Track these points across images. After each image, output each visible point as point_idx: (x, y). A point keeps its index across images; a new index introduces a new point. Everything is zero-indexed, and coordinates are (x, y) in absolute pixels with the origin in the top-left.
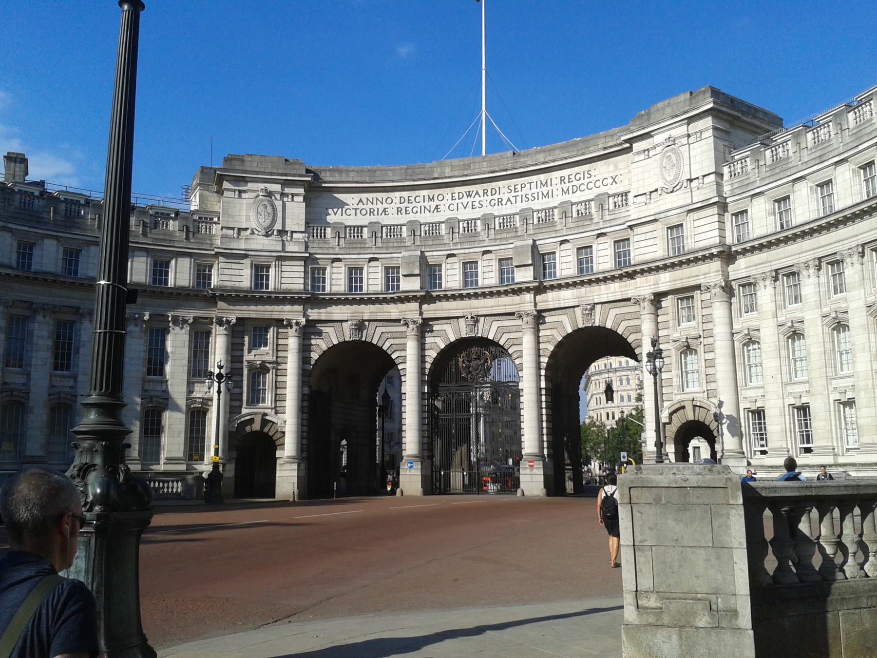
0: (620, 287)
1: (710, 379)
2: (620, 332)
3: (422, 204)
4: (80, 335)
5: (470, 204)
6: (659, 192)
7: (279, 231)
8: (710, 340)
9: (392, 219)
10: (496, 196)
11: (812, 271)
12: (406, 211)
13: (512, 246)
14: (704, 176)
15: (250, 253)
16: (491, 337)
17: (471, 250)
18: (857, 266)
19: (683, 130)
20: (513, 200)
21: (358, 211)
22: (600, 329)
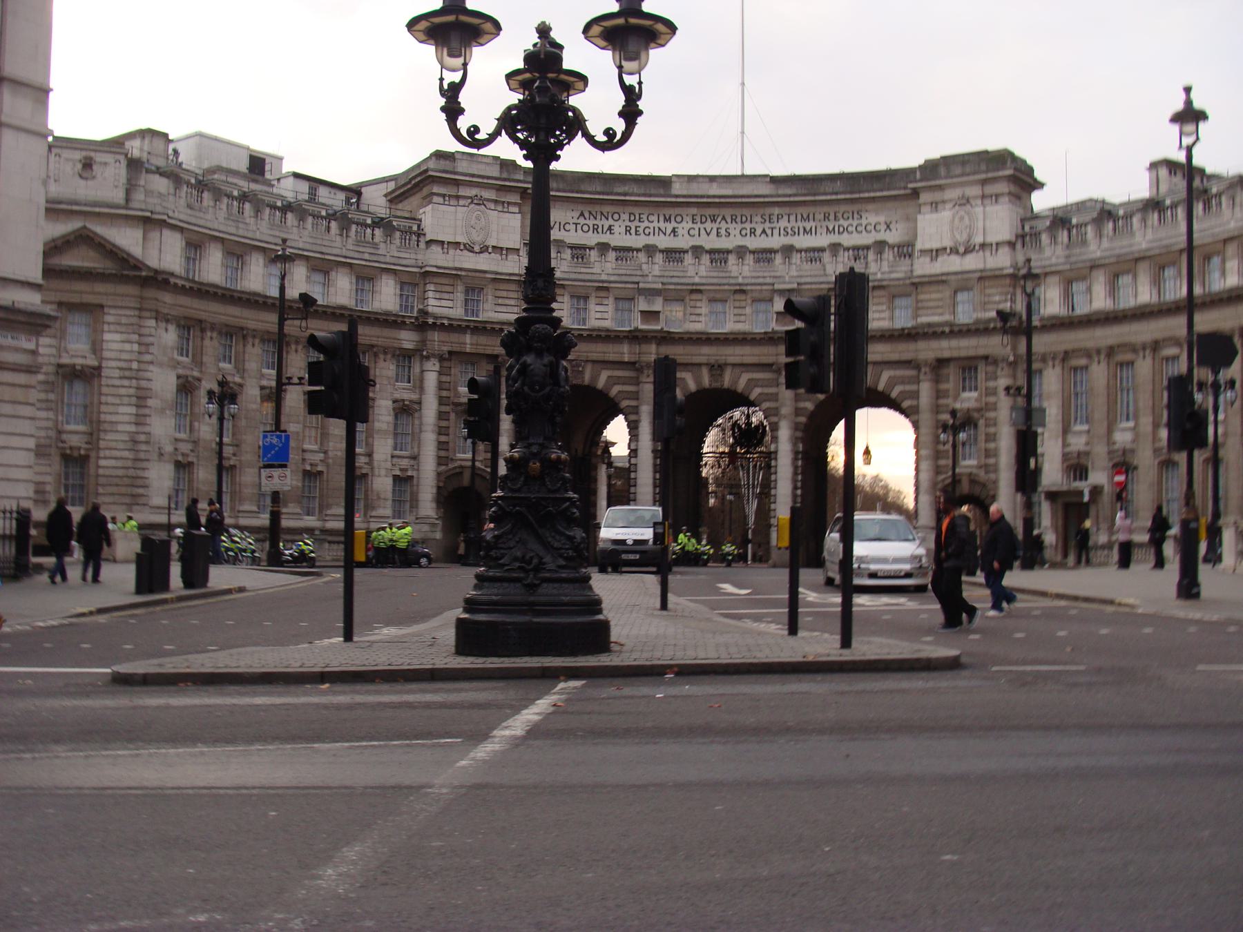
1: (993, 453)
3: (656, 224)
5: (714, 231)
7: (494, 247)
8: (991, 414)
9: (619, 238)
10: (748, 226)
11: (1102, 357)
12: (636, 231)
13: (770, 287)
14: (997, 244)
20: (769, 232)
21: (579, 227)
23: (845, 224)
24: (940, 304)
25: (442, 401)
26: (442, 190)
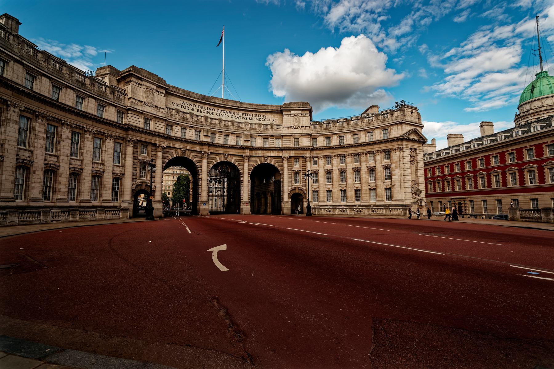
0: (277, 153)
2: (276, 166)
3: (206, 110)
4: (61, 135)
5: (224, 115)
6: (292, 128)
7: (155, 106)
9: (196, 113)
10: (234, 115)
11: (336, 157)
14: (306, 127)
15: (144, 112)
16: (232, 162)
17: (228, 131)
18: (350, 158)
19: (300, 112)
20: (239, 117)
21: (182, 106)
22: (270, 164)
23: (262, 118)
24: (290, 141)
25: (134, 158)
26: (136, 81)
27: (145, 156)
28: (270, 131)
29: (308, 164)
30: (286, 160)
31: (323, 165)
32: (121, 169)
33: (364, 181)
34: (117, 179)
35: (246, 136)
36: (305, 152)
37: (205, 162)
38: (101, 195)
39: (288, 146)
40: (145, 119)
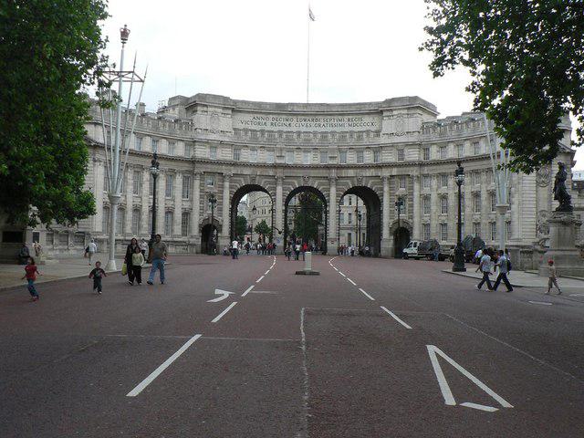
19: (406, 111)
27: (210, 188)
28: (366, 141)
29: (416, 186)
30: (386, 182)
31: (435, 187)
32: (189, 204)
33: (483, 211)
34: (186, 214)
35: (333, 150)
36: (412, 168)
37: (279, 190)
38: (172, 231)
39: (388, 161)
40: (211, 147)
